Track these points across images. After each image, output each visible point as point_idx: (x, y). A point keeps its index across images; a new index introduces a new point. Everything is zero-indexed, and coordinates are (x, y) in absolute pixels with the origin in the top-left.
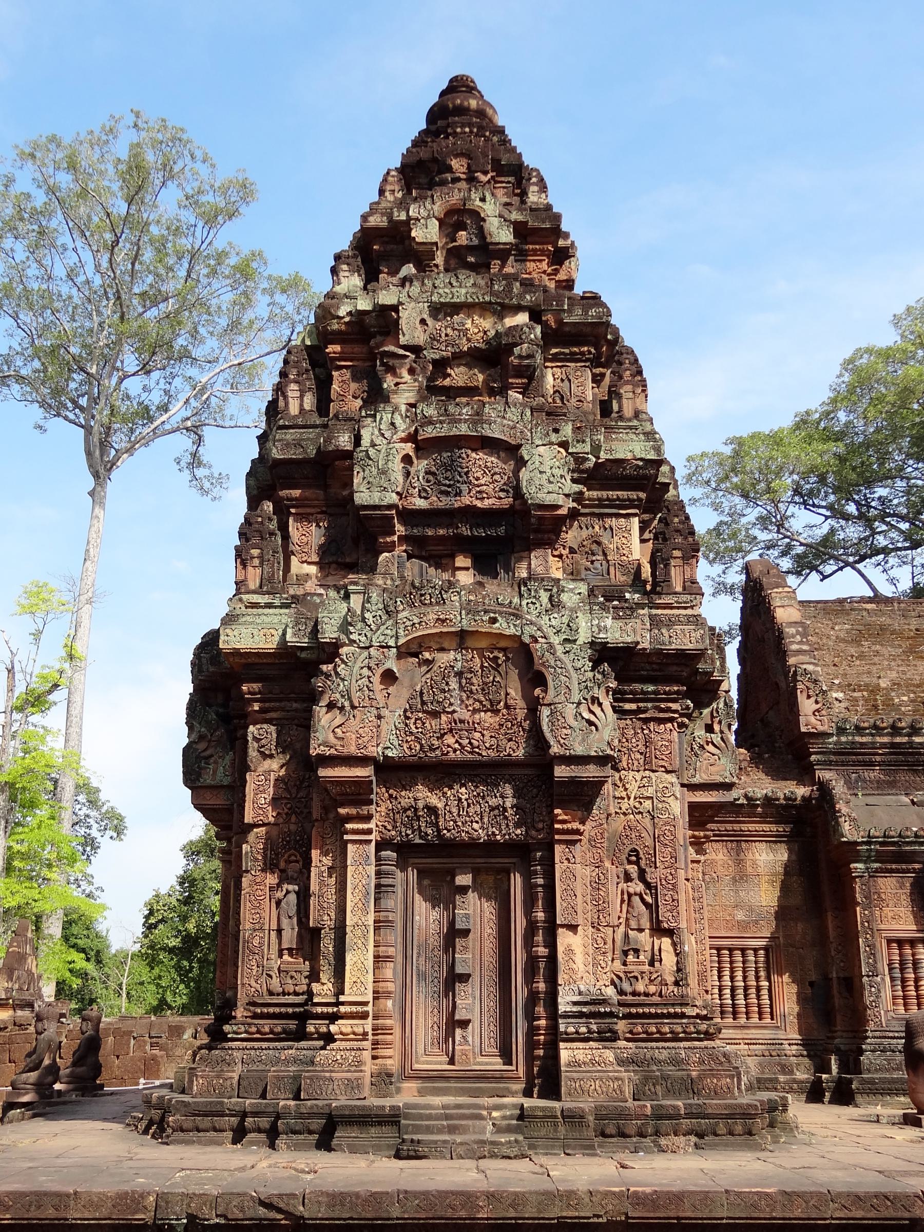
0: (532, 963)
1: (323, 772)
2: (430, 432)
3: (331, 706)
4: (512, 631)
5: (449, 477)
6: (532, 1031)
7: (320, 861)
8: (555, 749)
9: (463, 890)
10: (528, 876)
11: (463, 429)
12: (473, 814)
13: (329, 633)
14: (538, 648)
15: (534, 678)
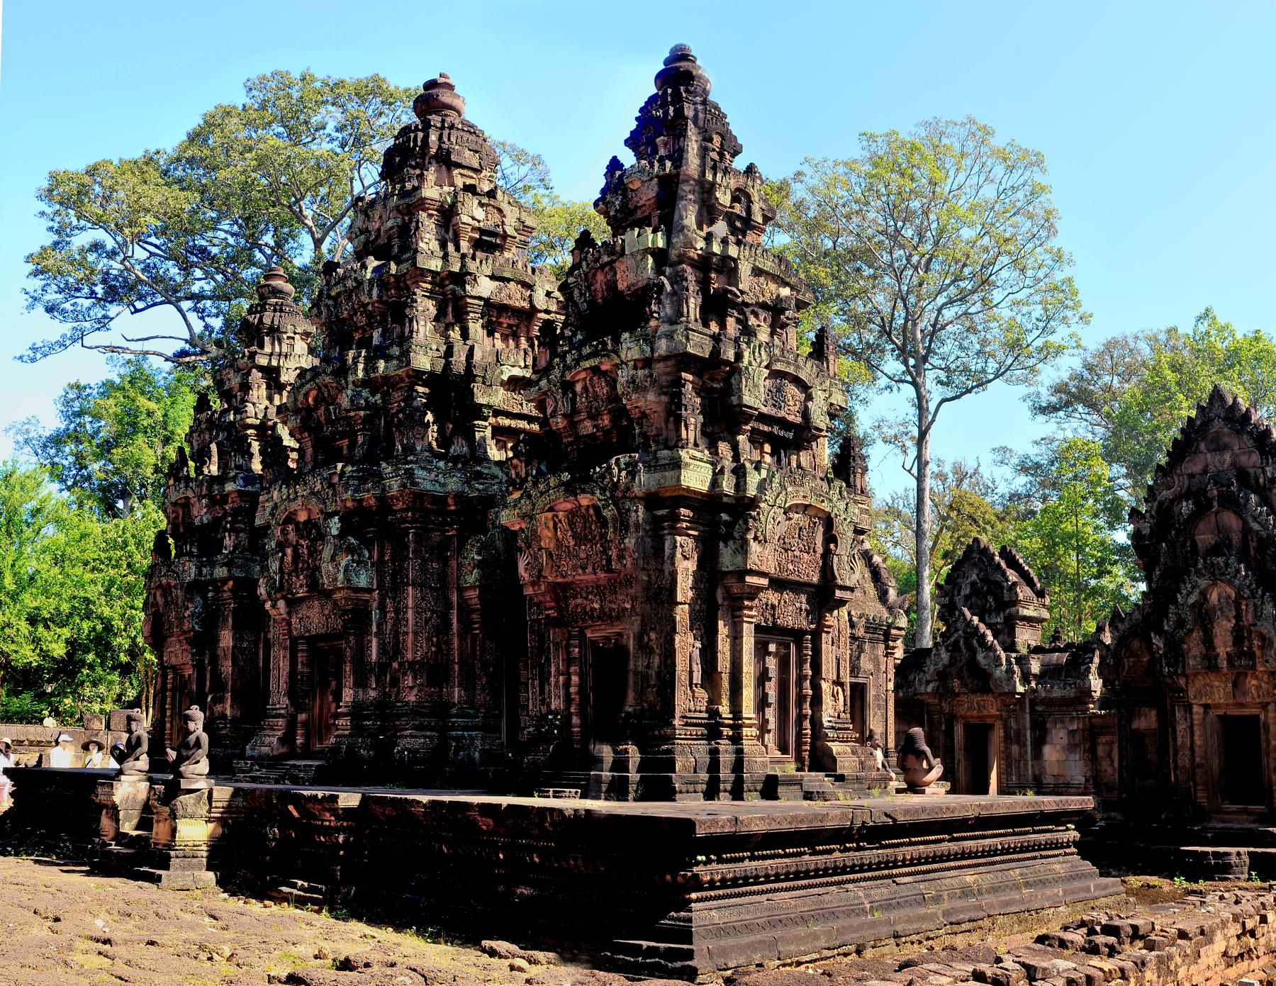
0: (801, 699)
1: (748, 579)
2: (778, 366)
3: (756, 538)
4: (828, 509)
5: (776, 395)
6: (800, 735)
7: (723, 629)
8: (839, 582)
9: (769, 654)
10: (800, 649)
11: (791, 370)
12: (793, 611)
13: (752, 491)
14: (837, 521)
15: (830, 538)
